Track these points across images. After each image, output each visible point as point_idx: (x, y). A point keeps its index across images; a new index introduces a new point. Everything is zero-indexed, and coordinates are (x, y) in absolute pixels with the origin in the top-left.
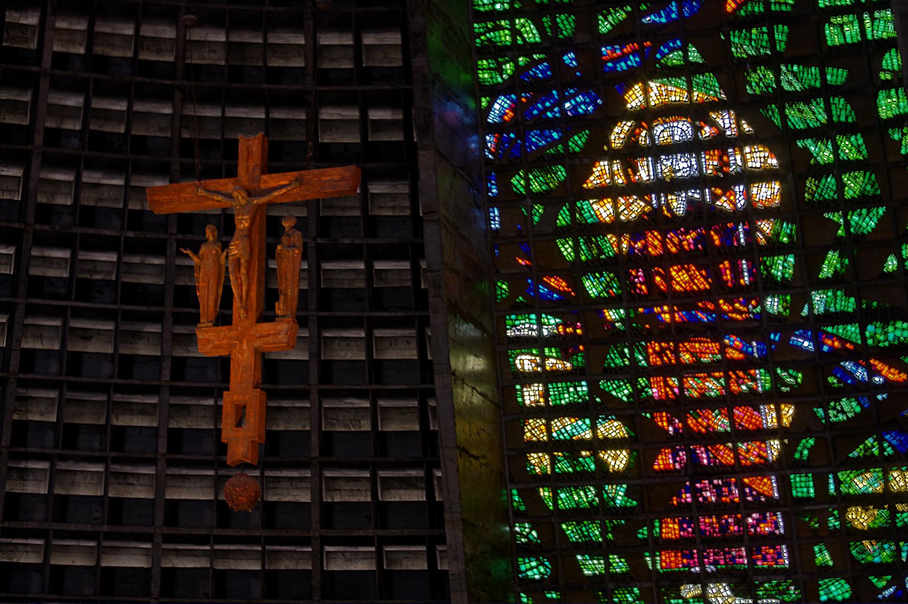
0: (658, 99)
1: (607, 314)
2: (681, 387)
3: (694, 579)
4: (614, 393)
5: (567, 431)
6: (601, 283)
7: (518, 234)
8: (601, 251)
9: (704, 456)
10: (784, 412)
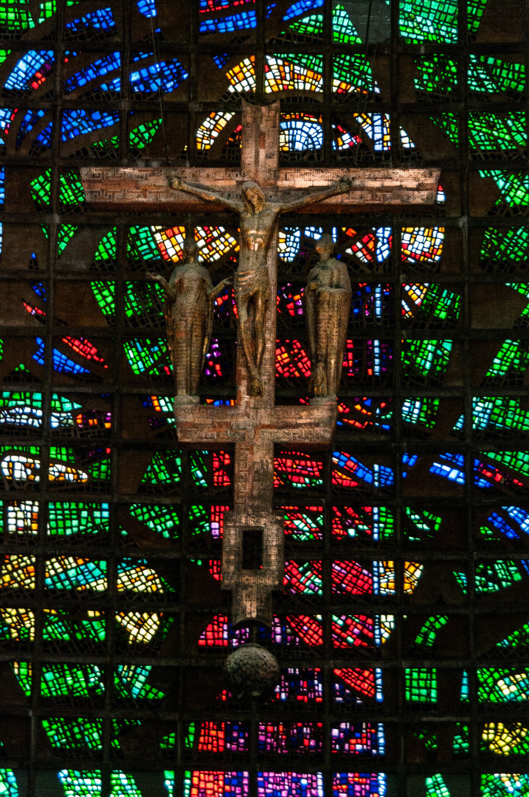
0: (277, 84)
1: (156, 403)
4: (151, 525)
5: (68, 578)
6: (151, 354)
7: (31, 267)
9: (278, 630)
10: (407, 574)
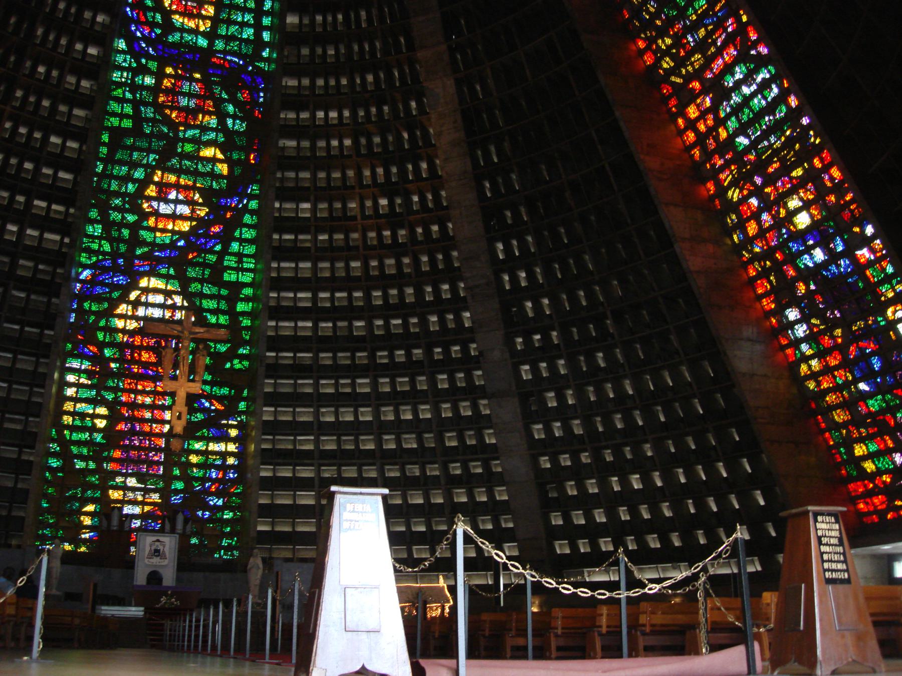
2: (135, 398)
3: (123, 475)
8: (115, 339)
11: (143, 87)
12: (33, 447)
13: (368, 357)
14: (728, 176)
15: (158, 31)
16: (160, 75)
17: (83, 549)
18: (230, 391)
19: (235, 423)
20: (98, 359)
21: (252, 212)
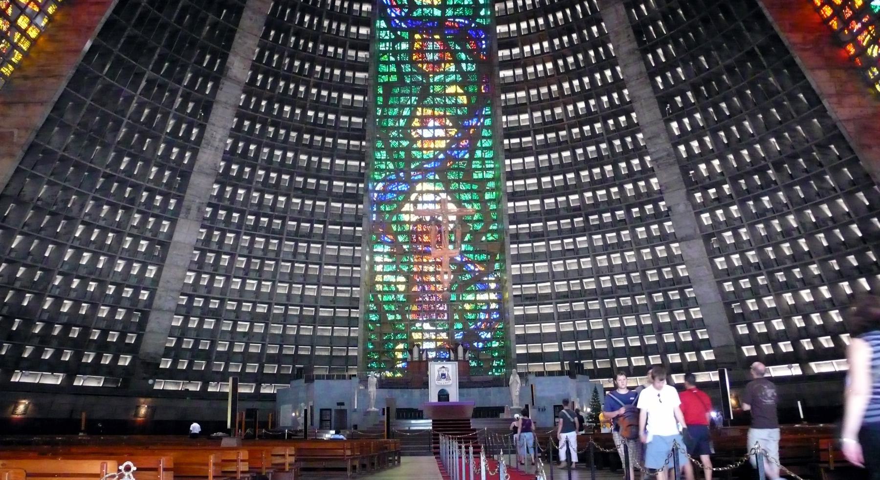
11: (401, 52)
12: (357, 308)
13: (583, 221)
14: (866, 36)
15: (406, 10)
16: (412, 41)
17: (399, 375)
18: (487, 257)
19: (493, 279)
20: (394, 243)
21: (488, 128)
